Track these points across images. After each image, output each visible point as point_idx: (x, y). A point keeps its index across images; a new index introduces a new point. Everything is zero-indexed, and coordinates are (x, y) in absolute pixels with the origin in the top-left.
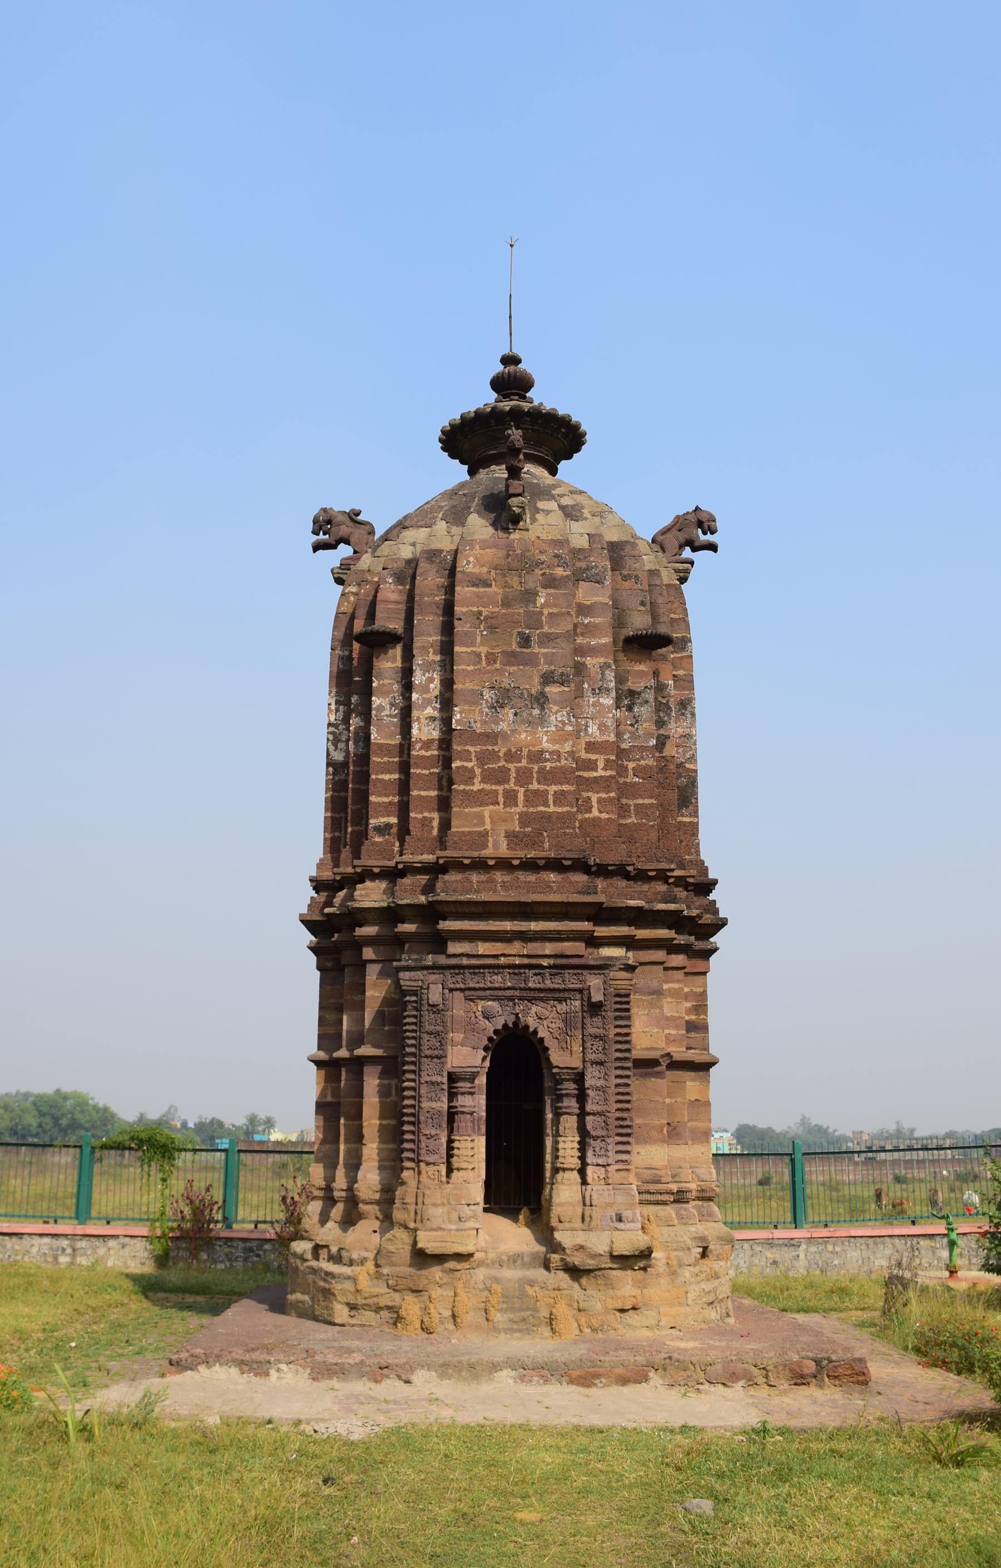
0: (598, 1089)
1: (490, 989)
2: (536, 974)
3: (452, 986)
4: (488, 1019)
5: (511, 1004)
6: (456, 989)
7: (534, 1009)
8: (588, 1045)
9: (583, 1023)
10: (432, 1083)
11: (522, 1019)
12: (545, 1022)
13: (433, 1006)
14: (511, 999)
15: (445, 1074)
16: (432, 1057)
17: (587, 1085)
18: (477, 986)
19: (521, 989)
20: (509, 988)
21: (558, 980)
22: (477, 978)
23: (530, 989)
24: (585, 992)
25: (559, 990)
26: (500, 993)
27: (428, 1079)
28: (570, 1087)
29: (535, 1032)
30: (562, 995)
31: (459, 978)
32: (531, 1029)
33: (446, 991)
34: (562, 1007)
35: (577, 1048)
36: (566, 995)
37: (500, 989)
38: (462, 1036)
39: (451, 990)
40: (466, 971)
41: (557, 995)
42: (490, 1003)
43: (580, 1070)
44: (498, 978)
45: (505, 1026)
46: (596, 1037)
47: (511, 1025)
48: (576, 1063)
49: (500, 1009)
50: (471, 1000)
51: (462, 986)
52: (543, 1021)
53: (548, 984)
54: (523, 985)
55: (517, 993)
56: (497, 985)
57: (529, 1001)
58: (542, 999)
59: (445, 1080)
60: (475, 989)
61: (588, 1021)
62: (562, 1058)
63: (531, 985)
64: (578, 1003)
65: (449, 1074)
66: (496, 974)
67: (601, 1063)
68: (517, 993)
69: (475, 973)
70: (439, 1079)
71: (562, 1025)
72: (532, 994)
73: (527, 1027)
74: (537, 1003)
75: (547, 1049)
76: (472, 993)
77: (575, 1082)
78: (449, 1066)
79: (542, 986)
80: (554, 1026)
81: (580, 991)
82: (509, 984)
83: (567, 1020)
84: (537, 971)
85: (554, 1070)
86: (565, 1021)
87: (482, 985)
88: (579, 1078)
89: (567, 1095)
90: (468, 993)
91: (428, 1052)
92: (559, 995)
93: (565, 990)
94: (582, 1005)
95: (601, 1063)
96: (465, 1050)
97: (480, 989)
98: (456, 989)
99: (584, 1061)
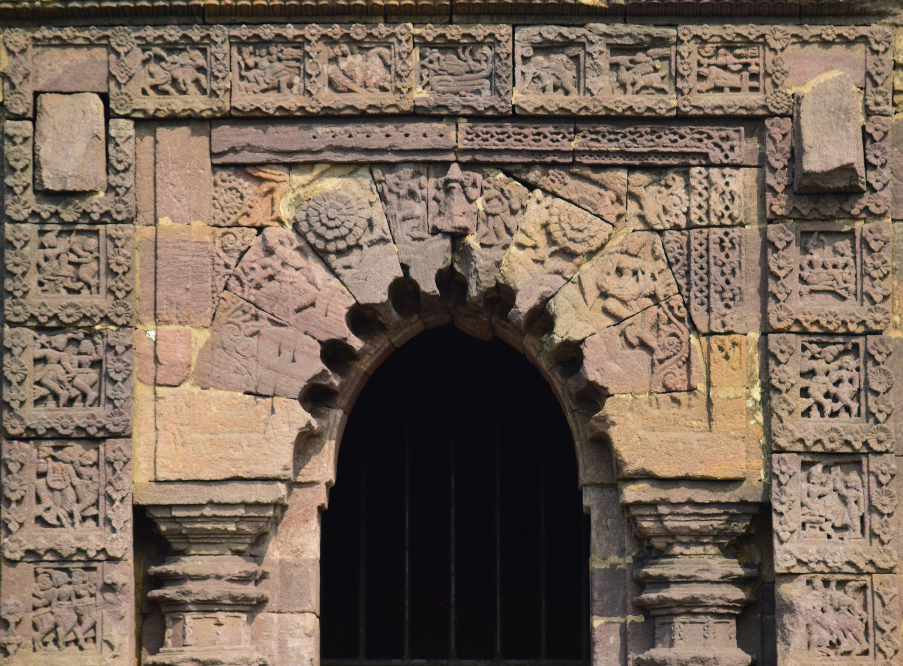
0: (834, 579)
1: (329, 117)
2: (544, 48)
3: (151, 104)
4: (321, 255)
5: (430, 185)
6: (173, 120)
7: (537, 210)
8: (788, 373)
9: (767, 274)
10: (62, 561)
11: (482, 259)
12: (590, 272)
13: (64, 196)
14: (431, 163)
15: (124, 515)
16: (59, 439)
17: (782, 561)
18: (270, 102)
19: (476, 117)
20: (418, 114)
21: (647, 70)
22: (268, 67)
23: (517, 117)
24: (777, 129)
25: (655, 121)
26: (377, 136)
27: (42, 539)
28: (704, 571)
29: (542, 317)
30: (666, 142)
31: (183, 67)
32: (524, 304)
33: (123, 128)
34: (666, 200)
35: (736, 387)
36: (689, 140)
37: (379, 117)
38: (202, 337)
39: (147, 123)
40: (219, 32)
41: (644, 145)
42: (331, 184)
43: (750, 492)
44: (367, 66)
45: (404, 289)
46: (826, 336)
47: (429, 286)
48: (729, 452)
49: (377, 212)
50: (240, 168)
51: (198, 103)
52: (575, 263)
53: (604, 91)
54: (483, 100)
55: (456, 136)
56: (362, 100)
57: (510, 171)
58: (571, 164)
59: (123, 542)
60: (257, 118)
61: (789, 259)
62: (664, 430)
63: (524, 97)
64: (742, 182)
65: (141, 513)
66: (360, 46)
67: (850, 459)
68: (456, 136)
69: (259, 43)
70: (93, 538)
71: (665, 285)
72: (528, 139)
73: (502, 295)
74: (554, 179)
75: (595, 396)
76: (250, 134)
77: (732, 546)
78: (139, 481)
79: (574, 102)
80: (627, 286)
81: (753, 123)
82: (420, 95)
83: (692, 261)
84: (551, 32)
85: (631, 493)
86: (681, 265)
87: (292, 101)
88: (750, 530)
89: (691, 607)
90: (226, 136)
91: (41, 417)
92: (651, 143)
93: (682, 119)
94: (764, 188)
95: (850, 459)
96: (221, 402)
97: (286, 118)
98: (173, 120)
99: (771, 449)
